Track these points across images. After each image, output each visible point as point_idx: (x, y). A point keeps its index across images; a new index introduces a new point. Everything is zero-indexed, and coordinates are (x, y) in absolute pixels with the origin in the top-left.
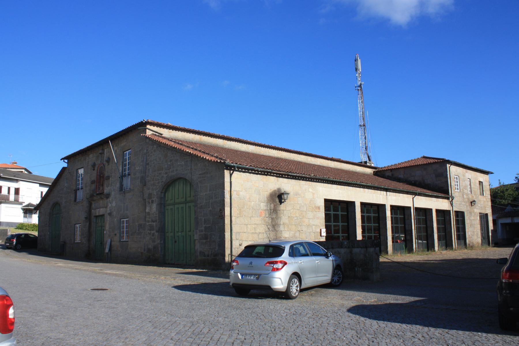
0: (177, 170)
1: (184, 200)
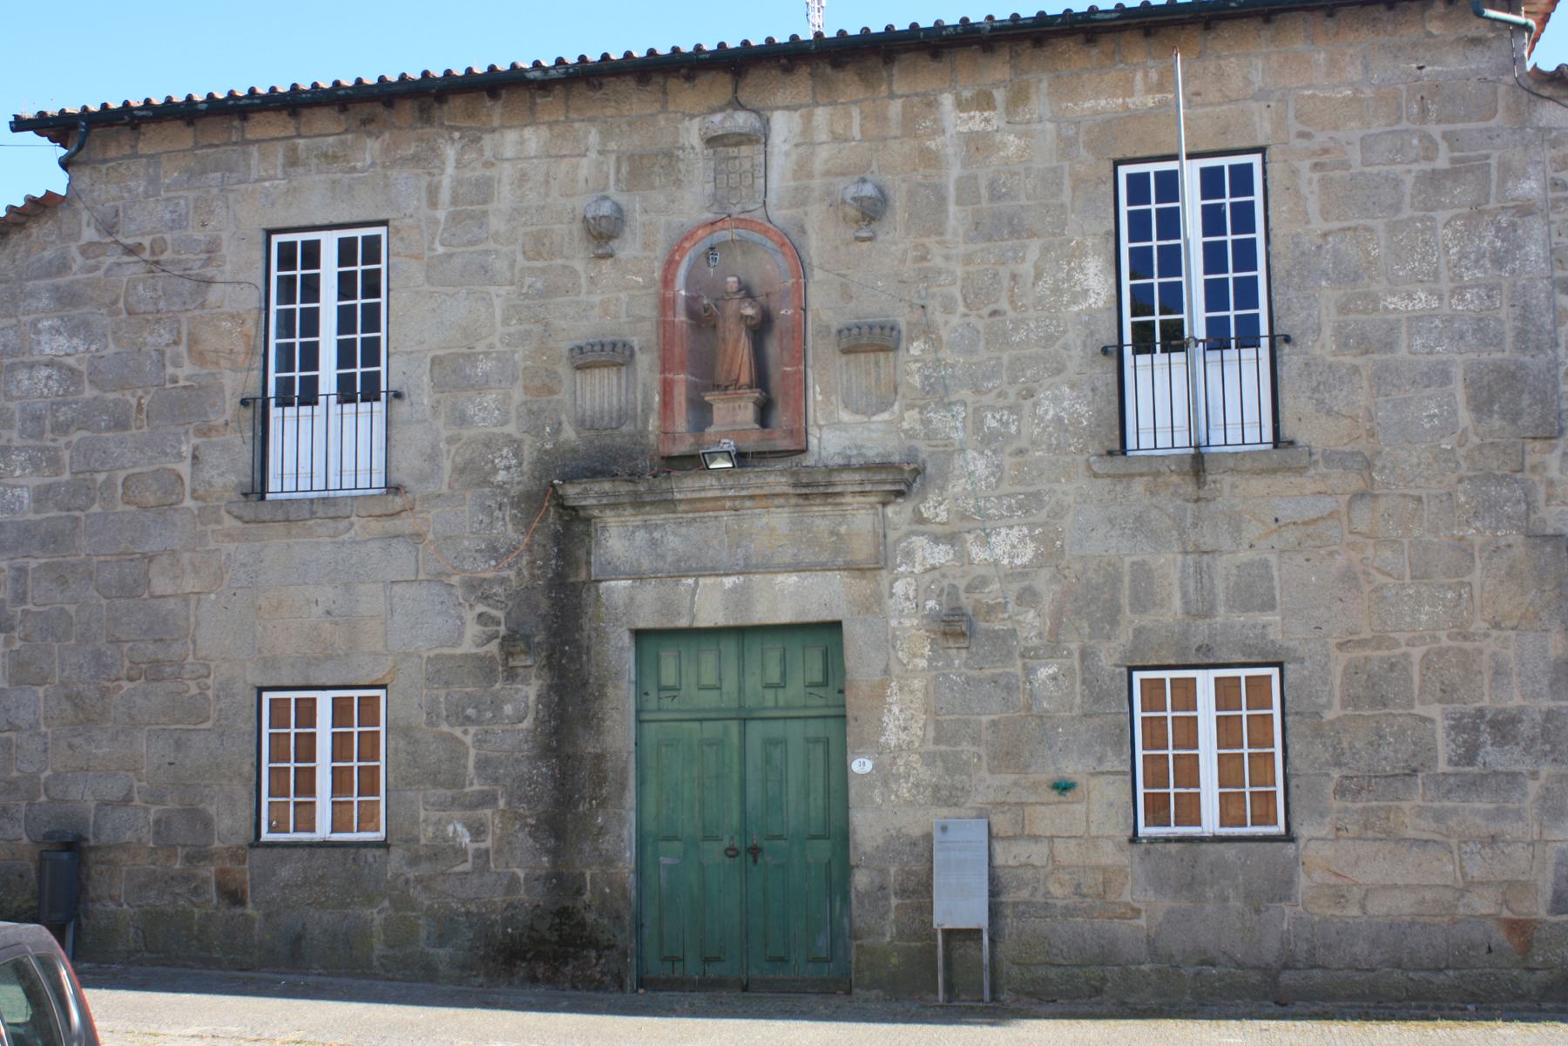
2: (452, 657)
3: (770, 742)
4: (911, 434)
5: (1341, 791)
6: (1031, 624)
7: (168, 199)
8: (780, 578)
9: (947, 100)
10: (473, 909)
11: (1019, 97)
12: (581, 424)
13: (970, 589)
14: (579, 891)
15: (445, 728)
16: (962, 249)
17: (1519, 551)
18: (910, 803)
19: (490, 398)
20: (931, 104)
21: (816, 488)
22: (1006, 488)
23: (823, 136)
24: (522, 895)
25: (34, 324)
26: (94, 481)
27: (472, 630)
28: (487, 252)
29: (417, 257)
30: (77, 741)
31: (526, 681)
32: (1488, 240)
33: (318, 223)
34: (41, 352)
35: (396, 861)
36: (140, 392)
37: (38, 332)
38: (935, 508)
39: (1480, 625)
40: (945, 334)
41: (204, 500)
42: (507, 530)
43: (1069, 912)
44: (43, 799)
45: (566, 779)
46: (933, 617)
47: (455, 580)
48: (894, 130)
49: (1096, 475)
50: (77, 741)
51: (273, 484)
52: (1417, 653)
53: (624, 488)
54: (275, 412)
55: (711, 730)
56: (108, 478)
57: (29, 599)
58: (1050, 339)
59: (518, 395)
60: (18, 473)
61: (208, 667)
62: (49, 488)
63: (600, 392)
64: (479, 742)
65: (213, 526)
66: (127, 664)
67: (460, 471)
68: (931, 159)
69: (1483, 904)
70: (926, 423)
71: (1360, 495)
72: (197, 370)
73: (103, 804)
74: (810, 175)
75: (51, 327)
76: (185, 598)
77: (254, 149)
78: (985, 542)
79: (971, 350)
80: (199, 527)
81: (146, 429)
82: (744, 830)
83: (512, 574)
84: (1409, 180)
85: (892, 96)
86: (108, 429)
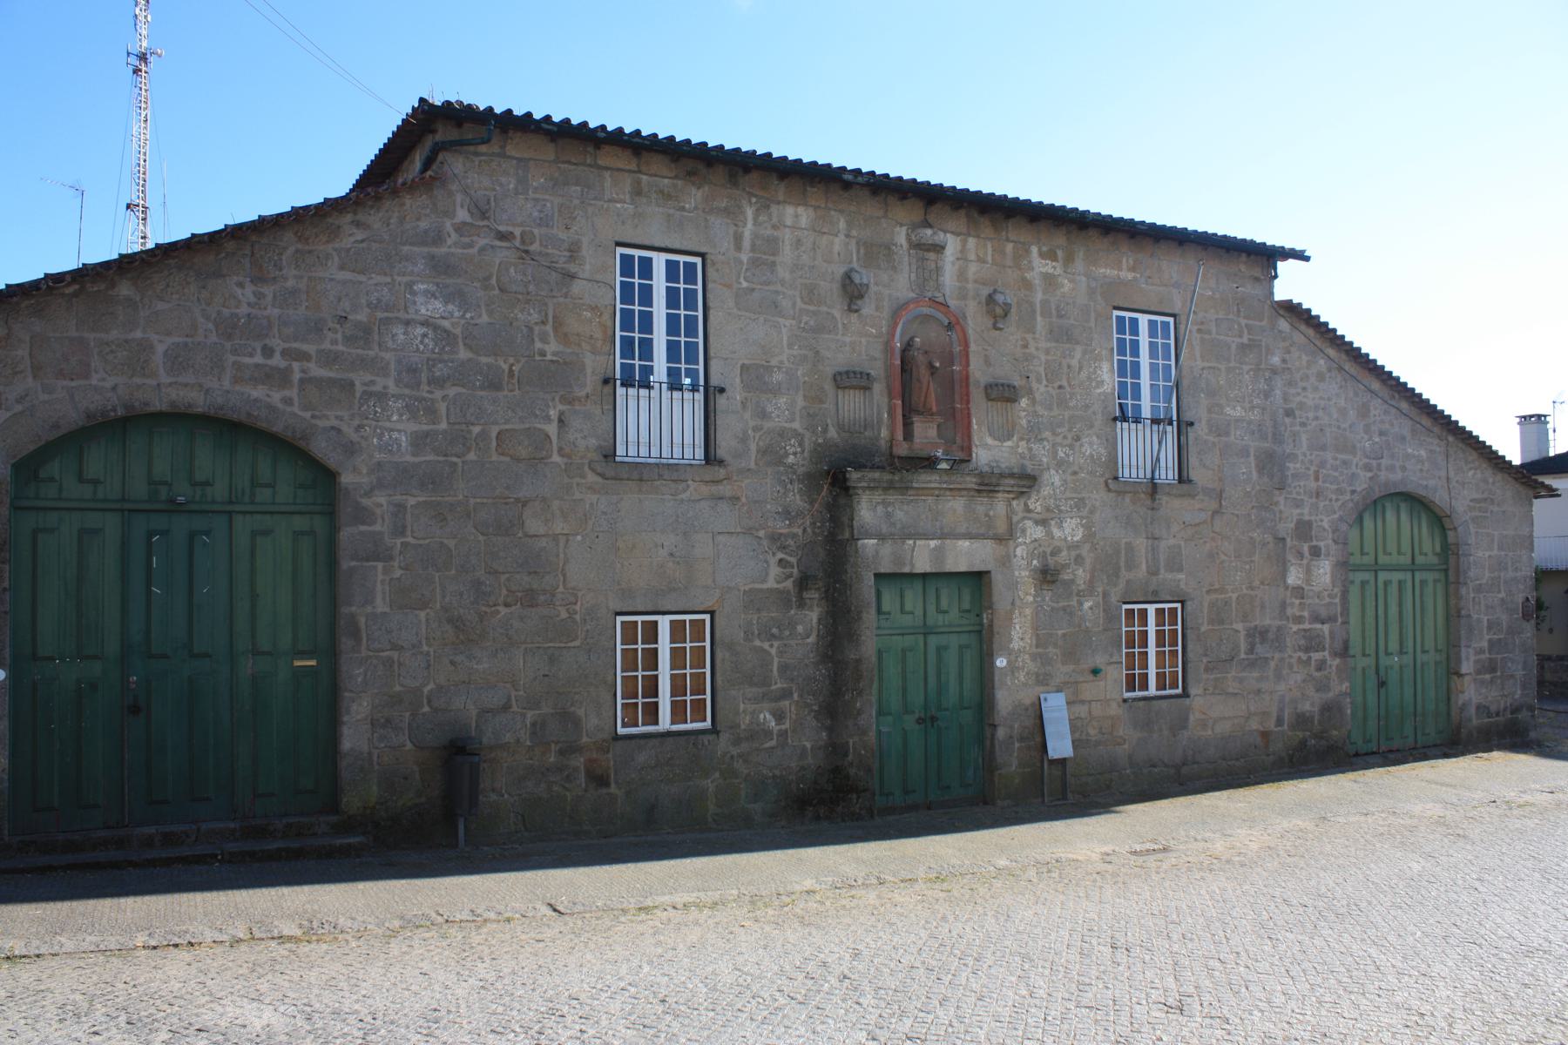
0: (1403, 468)
1: (1405, 560)
2: (761, 590)
3: (940, 650)
4: (1022, 456)
5: (1207, 670)
6: (1081, 575)
7: (536, 200)
8: (960, 542)
9: (1034, 250)
10: (777, 772)
11: (1069, 259)
12: (841, 427)
13: (1053, 554)
14: (846, 755)
15: (757, 643)
16: (1043, 345)
17: (1271, 546)
18: (1025, 685)
19: (782, 401)
20: (1028, 252)
21: (988, 484)
22: (1068, 494)
23: (972, 257)
24: (810, 760)
25: (410, 285)
26: (469, 432)
27: (775, 571)
28: (777, 292)
29: (729, 286)
30: (459, 658)
31: (811, 609)
32: (1262, 385)
33: (657, 244)
34: (417, 311)
35: (723, 743)
36: (511, 360)
37: (414, 293)
38: (1035, 504)
39: (1257, 583)
40: (1037, 396)
41: (569, 457)
42: (796, 500)
43: (1098, 743)
44: (426, 709)
45: (837, 675)
46: (1035, 570)
47: (761, 533)
48: (1009, 262)
49: (1109, 490)
50: (459, 658)
51: (620, 451)
52: (1234, 596)
53: (887, 477)
54: (620, 391)
55: (909, 640)
56: (483, 431)
58: (1087, 407)
59: (800, 402)
60: (395, 418)
61: (576, 596)
62: (427, 434)
63: (852, 405)
64: (781, 653)
65: (577, 480)
66: (504, 592)
67: (763, 452)
68: (1027, 285)
69: (1254, 725)
70: (1030, 450)
71: (1215, 513)
72: (561, 348)
73: (484, 712)
74: (966, 280)
75: (426, 292)
76: (555, 538)
77: (607, 174)
78: (1060, 526)
79: (1050, 409)
80: (566, 480)
81: (517, 392)
82: (926, 707)
83: (800, 531)
84: (1234, 346)
85: (1008, 240)
86: (482, 388)
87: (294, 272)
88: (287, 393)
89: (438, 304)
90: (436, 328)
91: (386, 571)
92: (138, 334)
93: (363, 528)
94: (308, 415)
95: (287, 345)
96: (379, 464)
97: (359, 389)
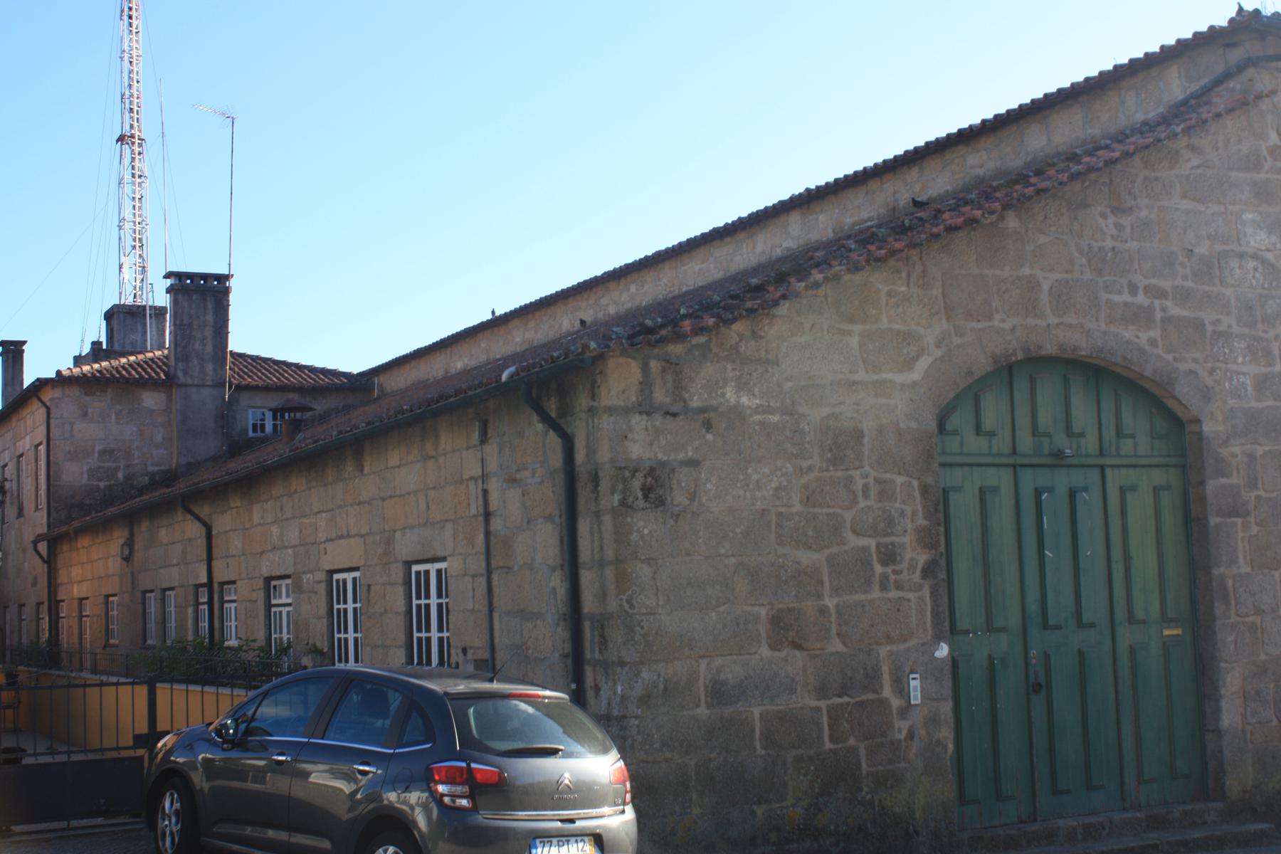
34: (1248, 243)
57: (1260, 486)
60: (1240, 360)
87: (1146, 201)
88: (1151, 334)
89: (1263, 235)
90: (1264, 262)
91: (1246, 527)
92: (1026, 271)
93: (1224, 481)
94: (1170, 357)
95: (1147, 282)
96: (1232, 410)
97: (1209, 328)
